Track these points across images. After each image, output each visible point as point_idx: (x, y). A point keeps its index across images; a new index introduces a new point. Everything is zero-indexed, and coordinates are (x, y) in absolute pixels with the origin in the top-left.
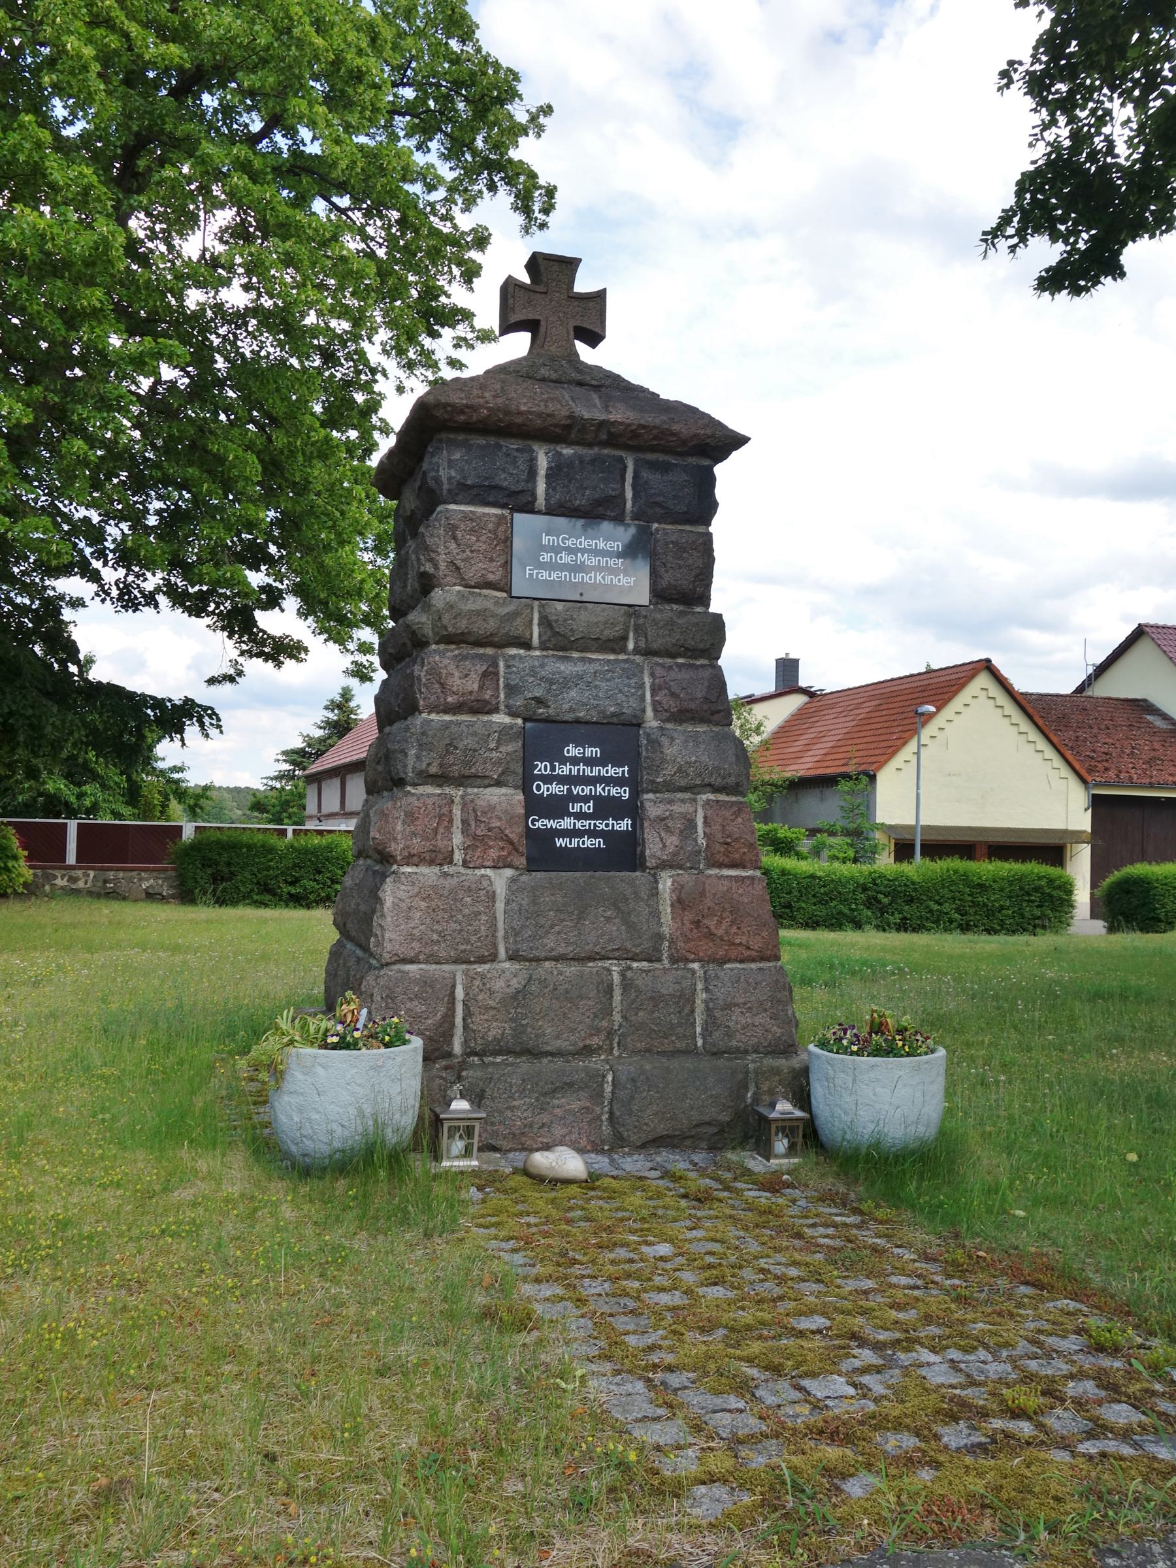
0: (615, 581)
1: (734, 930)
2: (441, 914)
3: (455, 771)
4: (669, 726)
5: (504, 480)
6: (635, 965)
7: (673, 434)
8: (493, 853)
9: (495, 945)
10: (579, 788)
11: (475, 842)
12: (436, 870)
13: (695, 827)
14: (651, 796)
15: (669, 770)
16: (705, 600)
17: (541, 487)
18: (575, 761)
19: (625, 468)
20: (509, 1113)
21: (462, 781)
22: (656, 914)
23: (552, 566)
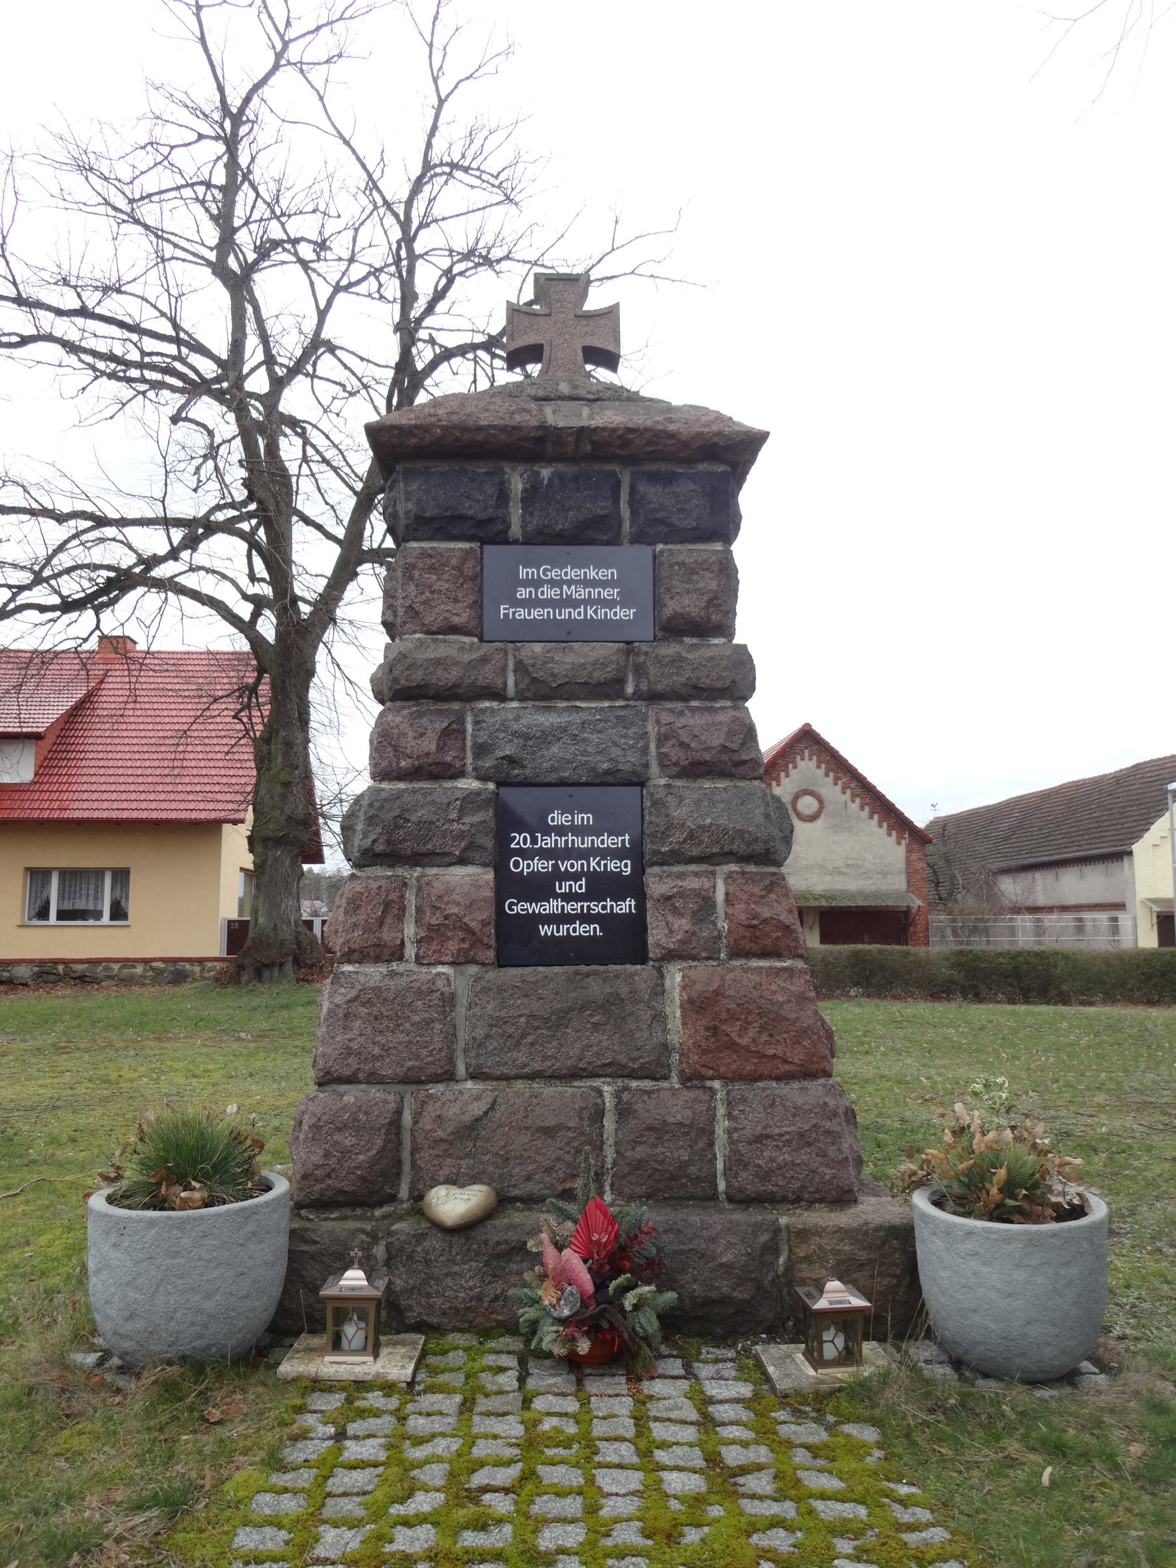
0: (610, 615)
1: (765, 1037)
2: (385, 1022)
3: (408, 847)
4: (679, 783)
5: (470, 508)
6: (634, 1084)
7: (672, 435)
8: (453, 946)
9: (451, 1061)
11: (432, 935)
12: (383, 969)
14: (656, 869)
16: (726, 629)
17: (516, 513)
18: (561, 831)
19: (618, 483)
21: (417, 859)
22: (660, 1018)
23: (530, 603)
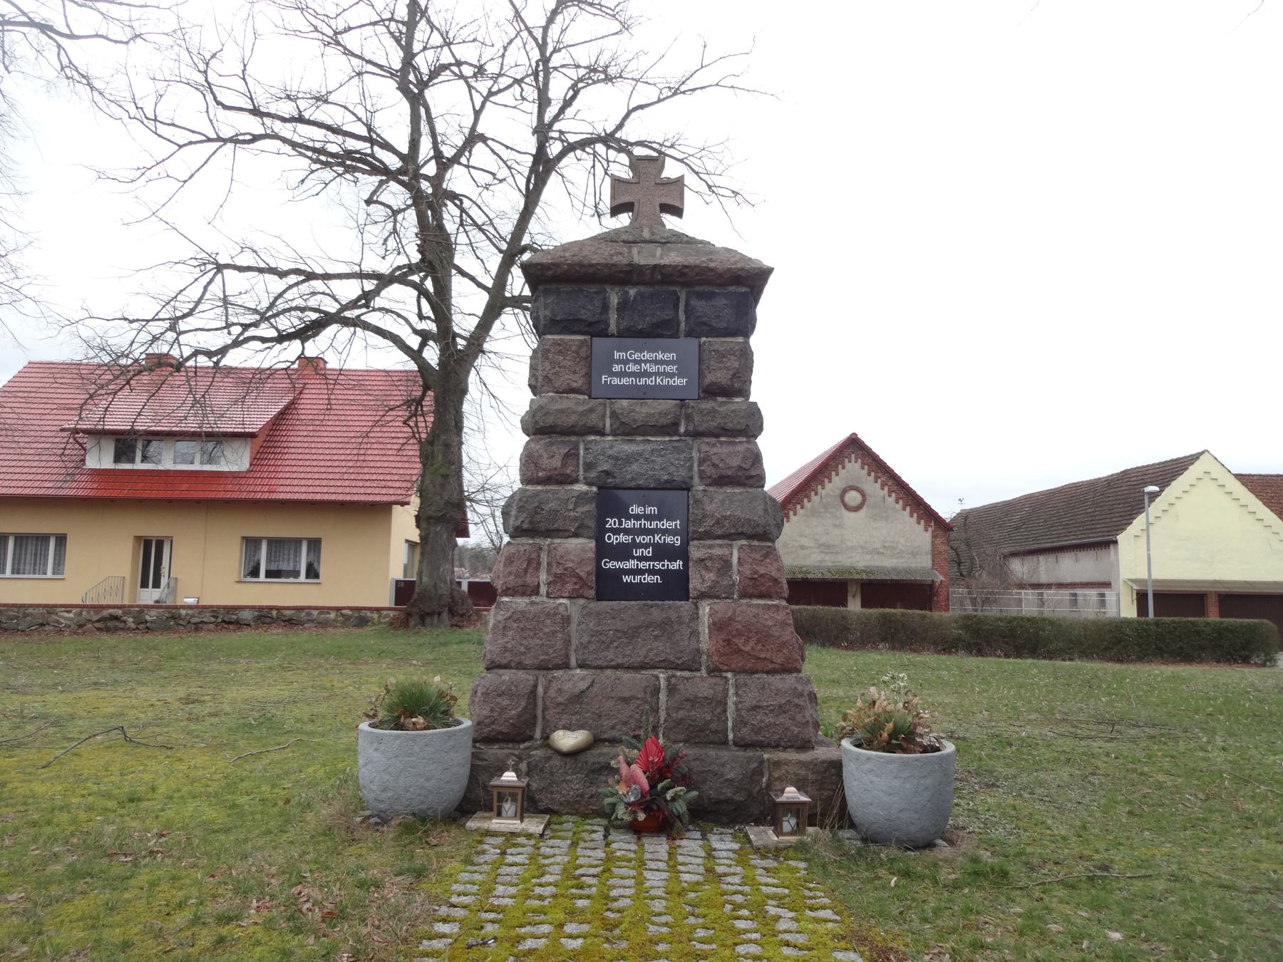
0: (671, 382)
1: (759, 647)
2: (528, 632)
3: (542, 526)
4: (711, 489)
5: (585, 315)
6: (678, 673)
7: (712, 270)
8: (569, 587)
9: (567, 656)
10: (641, 538)
11: (557, 580)
12: (526, 600)
13: (731, 566)
14: (696, 542)
15: (709, 522)
16: (744, 392)
17: (613, 317)
18: (637, 517)
19: (678, 299)
20: (565, 785)
21: (548, 533)
22: (695, 634)
23: (621, 374)
